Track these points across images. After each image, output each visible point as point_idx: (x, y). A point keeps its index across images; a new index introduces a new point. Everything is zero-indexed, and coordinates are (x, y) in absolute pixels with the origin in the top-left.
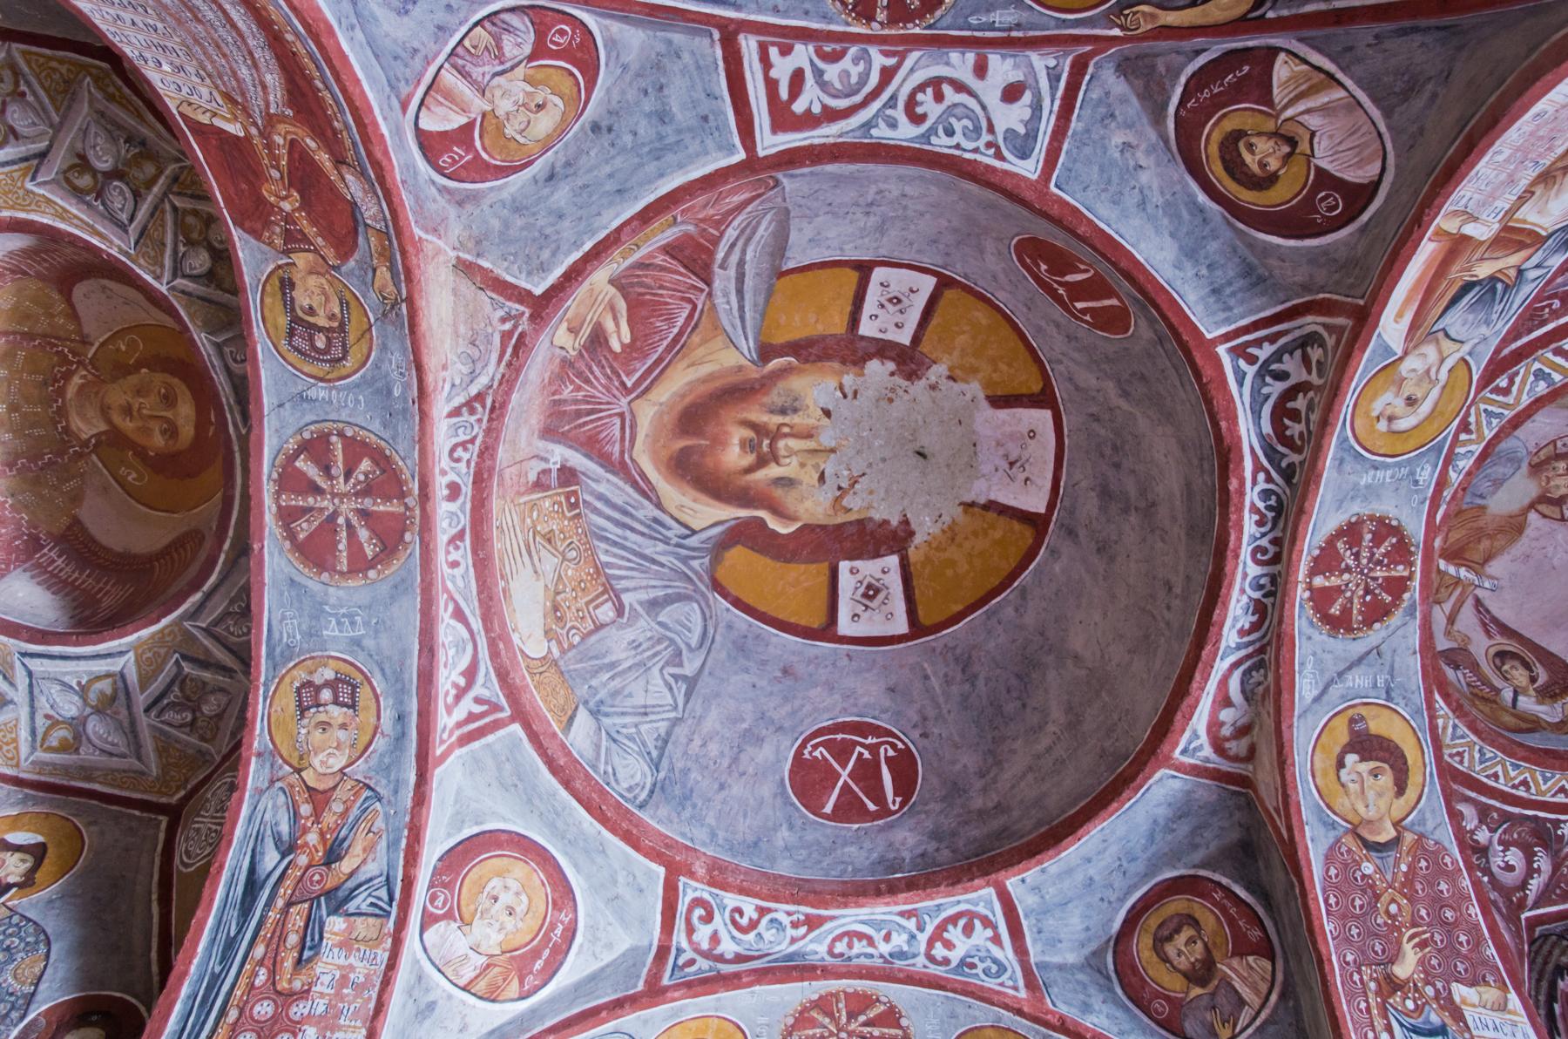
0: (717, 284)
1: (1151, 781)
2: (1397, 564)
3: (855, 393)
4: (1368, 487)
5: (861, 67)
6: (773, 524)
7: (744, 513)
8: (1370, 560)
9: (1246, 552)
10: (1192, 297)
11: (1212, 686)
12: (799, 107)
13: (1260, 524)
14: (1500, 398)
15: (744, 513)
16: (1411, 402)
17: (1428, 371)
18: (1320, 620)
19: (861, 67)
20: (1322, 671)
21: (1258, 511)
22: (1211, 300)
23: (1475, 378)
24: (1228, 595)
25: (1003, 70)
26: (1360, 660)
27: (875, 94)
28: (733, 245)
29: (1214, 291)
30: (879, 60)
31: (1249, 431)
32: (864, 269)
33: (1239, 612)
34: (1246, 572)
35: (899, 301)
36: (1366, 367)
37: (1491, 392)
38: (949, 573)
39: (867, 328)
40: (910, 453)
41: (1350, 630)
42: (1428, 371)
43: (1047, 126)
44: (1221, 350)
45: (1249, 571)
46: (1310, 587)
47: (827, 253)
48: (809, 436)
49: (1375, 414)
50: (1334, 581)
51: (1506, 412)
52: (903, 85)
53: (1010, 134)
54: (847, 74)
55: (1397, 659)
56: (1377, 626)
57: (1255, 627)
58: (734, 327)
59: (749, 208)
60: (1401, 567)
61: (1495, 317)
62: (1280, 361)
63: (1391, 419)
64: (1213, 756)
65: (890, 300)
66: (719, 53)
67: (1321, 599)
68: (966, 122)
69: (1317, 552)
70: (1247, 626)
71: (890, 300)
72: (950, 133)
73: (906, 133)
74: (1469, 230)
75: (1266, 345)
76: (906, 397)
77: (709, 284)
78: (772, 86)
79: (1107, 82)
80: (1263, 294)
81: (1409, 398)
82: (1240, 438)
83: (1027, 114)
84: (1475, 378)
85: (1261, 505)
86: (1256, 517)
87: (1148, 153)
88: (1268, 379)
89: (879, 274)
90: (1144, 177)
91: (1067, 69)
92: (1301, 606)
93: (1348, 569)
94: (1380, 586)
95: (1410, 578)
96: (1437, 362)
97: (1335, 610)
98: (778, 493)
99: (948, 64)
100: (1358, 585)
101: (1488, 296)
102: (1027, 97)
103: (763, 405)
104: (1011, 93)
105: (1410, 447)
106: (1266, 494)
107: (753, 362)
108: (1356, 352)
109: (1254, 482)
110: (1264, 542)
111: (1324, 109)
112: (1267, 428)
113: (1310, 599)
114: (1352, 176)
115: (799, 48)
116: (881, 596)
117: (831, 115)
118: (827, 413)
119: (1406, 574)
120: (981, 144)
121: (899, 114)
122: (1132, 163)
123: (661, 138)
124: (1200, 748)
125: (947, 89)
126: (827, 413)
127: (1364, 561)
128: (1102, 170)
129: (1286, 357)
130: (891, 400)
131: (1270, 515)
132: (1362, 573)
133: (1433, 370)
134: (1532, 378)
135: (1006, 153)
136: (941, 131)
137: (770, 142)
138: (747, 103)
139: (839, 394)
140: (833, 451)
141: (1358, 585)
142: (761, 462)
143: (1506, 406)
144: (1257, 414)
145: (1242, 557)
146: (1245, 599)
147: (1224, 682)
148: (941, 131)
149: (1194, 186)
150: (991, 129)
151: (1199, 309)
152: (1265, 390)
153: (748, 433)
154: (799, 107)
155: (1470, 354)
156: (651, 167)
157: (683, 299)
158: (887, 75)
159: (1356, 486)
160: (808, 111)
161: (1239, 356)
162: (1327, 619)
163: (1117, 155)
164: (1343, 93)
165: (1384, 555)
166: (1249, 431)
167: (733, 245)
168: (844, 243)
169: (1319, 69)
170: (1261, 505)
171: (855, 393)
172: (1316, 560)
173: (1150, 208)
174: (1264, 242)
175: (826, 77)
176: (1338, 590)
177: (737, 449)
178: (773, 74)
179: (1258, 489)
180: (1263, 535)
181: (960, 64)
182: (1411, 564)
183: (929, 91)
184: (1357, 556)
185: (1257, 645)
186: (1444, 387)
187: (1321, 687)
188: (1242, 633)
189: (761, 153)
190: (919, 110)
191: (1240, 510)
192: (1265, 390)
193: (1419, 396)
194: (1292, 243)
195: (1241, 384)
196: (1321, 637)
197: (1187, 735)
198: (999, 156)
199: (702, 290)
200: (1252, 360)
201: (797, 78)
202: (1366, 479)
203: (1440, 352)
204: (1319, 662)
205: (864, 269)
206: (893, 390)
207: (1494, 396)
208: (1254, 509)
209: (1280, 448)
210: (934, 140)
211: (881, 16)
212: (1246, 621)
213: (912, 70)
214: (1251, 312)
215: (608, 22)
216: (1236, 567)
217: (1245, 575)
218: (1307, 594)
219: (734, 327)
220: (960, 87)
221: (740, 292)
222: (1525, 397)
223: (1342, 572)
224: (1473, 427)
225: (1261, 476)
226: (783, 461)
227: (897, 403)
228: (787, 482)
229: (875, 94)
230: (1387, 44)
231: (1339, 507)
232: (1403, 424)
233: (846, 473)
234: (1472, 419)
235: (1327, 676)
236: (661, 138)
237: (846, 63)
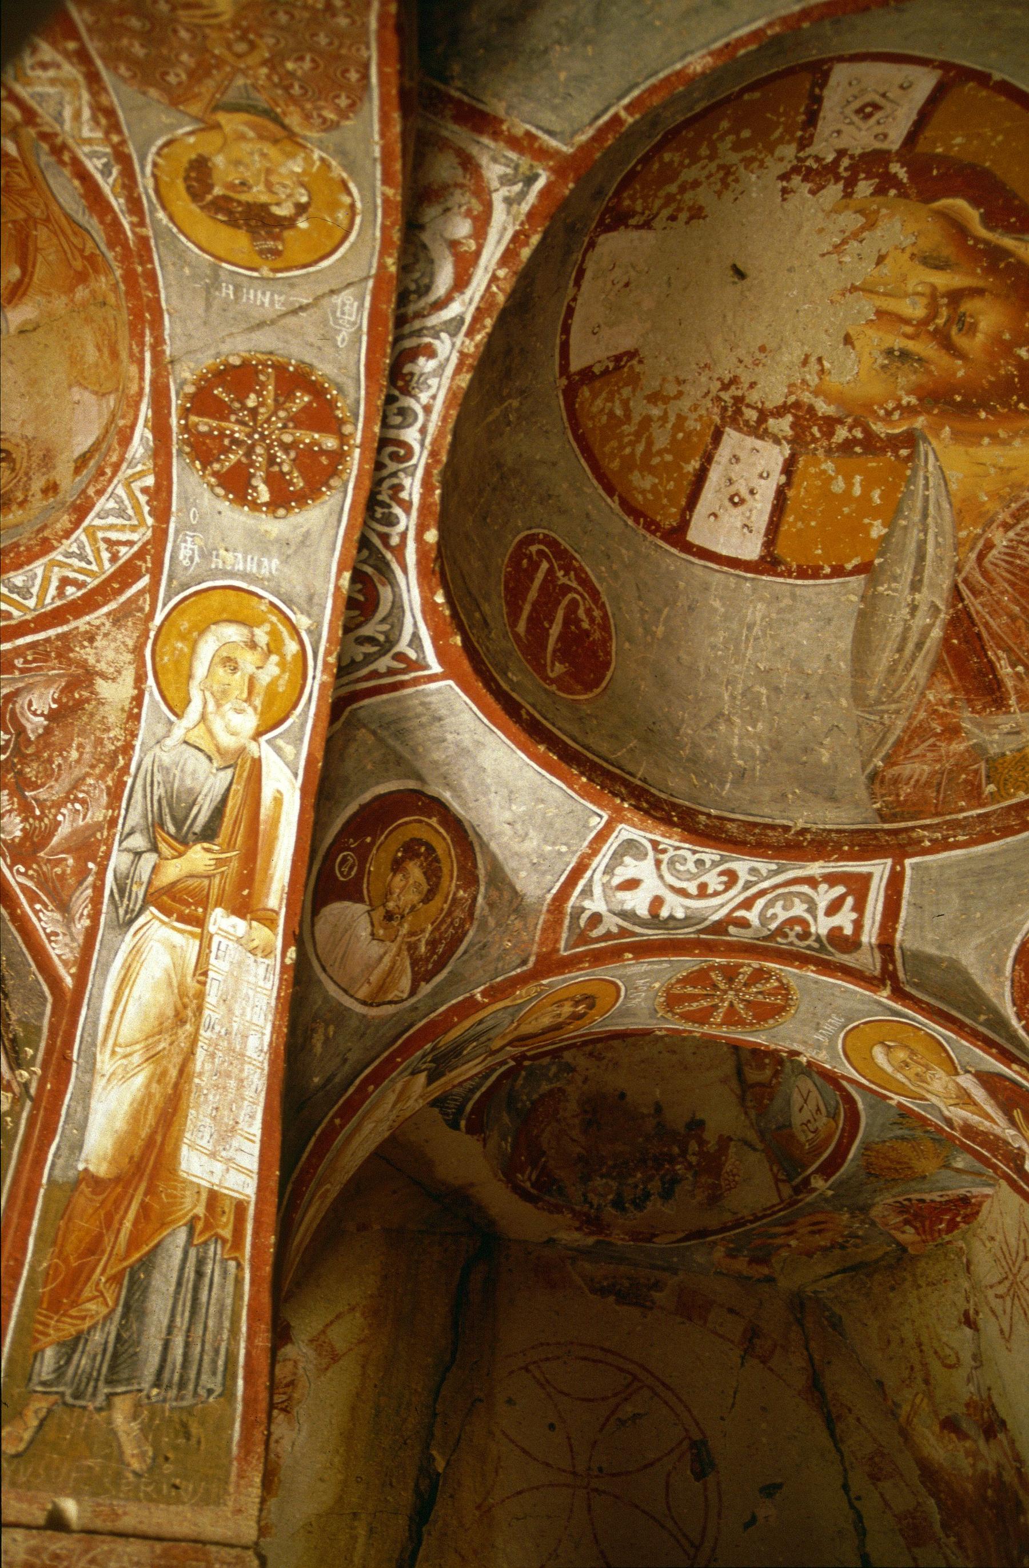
0: (946, 585)
1: (590, 132)
2: (209, 434)
3: (805, 363)
4: (265, 552)
5: (770, 912)
6: (972, 215)
7: (1008, 242)
8: (250, 451)
9: (420, 459)
10: (467, 716)
11: (480, 280)
12: (840, 890)
13: (398, 488)
14: (72, 575)
15: (1008, 242)
16: (231, 663)
17: (219, 705)
18: (326, 391)
19: (770, 912)
20: (325, 322)
21: (401, 503)
22: (443, 712)
23: (151, 681)
24: (448, 406)
25: (638, 902)
26: (261, 325)
27: (762, 893)
28: (919, 646)
29: (440, 719)
30: (752, 916)
31: (409, 588)
32: (769, 563)
33: (433, 382)
34: (424, 432)
35: (731, 499)
36: (303, 725)
37: (84, 584)
38: (746, 134)
39: (772, 457)
40: (751, 273)
41: (280, 369)
42: (219, 705)
43: (600, 861)
44: (436, 668)
45: (418, 436)
46: (343, 439)
47: (809, 593)
48: (880, 313)
49: (274, 658)
50: (307, 437)
51: (60, 558)
52: (736, 895)
53: (641, 856)
54: (784, 908)
55: (201, 311)
56: (235, 361)
57: (412, 355)
58: (939, 507)
59: (901, 723)
60: (204, 428)
61: (158, 777)
62: (366, 655)
63: (253, 645)
64: (484, 160)
65: (742, 501)
66: (898, 936)
67: (322, 415)
68: (681, 868)
69: (334, 482)
70: (422, 360)
71: (742, 501)
72: (700, 863)
73: (742, 866)
74: (239, 926)
75: (383, 670)
76: (741, 352)
77: (956, 587)
78: (859, 908)
79: (535, 885)
80: (384, 715)
81: (235, 670)
82: (420, 585)
83: (619, 870)
84: (151, 681)
85: (397, 510)
86: (404, 495)
87: (501, 833)
88: (382, 638)
89: (752, 550)
90: (507, 816)
91: (573, 899)
92: (356, 416)
93: (286, 448)
94: (234, 412)
95: (185, 413)
96: (210, 717)
97: (303, 399)
98: (948, 251)
99: (687, 908)
100: (268, 421)
101: (180, 815)
102: (616, 881)
103: (930, 373)
104: (632, 884)
105: (216, 596)
106: (391, 521)
107: (926, 440)
108: (320, 755)
109: (404, 535)
110: (392, 466)
111: (370, 968)
112: (386, 594)
113: (342, 422)
114: (337, 910)
115: (823, 931)
116: (857, 104)
117: (811, 882)
118: (848, 340)
119: (194, 419)
120: (671, 852)
121: (743, 876)
122: (518, 826)
123: (979, 882)
124: (506, 180)
125: (693, 890)
126: (848, 340)
127: (259, 450)
128: (551, 825)
129: (359, 658)
130: (762, 349)
131: (384, 497)
132: (263, 437)
133: (211, 706)
134: (35, 590)
135: (649, 846)
136: (708, 864)
137: (879, 869)
138: (888, 899)
139: (827, 365)
140: (854, 289)
141: (268, 421)
142: (955, 297)
143: (61, 565)
144: (397, 606)
145: (426, 453)
146: (424, 397)
147: (461, 283)
148: (708, 864)
149: (456, 806)
150: (658, 863)
151: (458, 706)
152: (385, 627)
153: (961, 341)
154: (840, 890)
155: (171, 723)
156: (998, 861)
157: (991, 582)
158: (747, 904)
159: (286, 560)
160: (832, 885)
161: (416, 662)
162: (317, 390)
163: (532, 833)
164: (360, 995)
165: (227, 451)
166: (409, 588)
167: (919, 646)
168: (791, 609)
169: (379, 1005)
170: (397, 510)
171: (805, 363)
172: (334, 473)
173: (505, 792)
174: (389, 779)
175: (805, 906)
176: (298, 421)
177: (983, 325)
178: (854, 916)
179: (401, 527)
180: (394, 474)
181: (675, 907)
182: (185, 429)
183: (710, 891)
184: (271, 460)
185: (407, 329)
186: (190, 677)
187: (324, 302)
188: (430, 353)
189: (889, 862)
190: (725, 879)
191: (424, 507)
192: (385, 627)
193: (220, 671)
194: (367, 797)
195: (416, 636)
196: (324, 369)
197: (525, 207)
198: (655, 844)
199: (965, 581)
200: (400, 657)
201: (834, 908)
202: (272, 565)
203: (210, 732)
204: (328, 338)
205: (769, 563)
206: (756, 363)
207: (81, 578)
208: (407, 506)
209: (369, 570)
210: (717, 858)
211: (748, 970)
212: (425, 365)
213: (722, 905)
214: (398, 700)
215: (995, 1000)
216: (434, 442)
217: (423, 431)
218: (347, 429)
219: (939, 507)
220: (683, 893)
221: (921, 557)
222: (40, 572)
223: (294, 445)
224: (103, 546)
225: (395, 541)
226: (928, 291)
227: (754, 348)
228: (933, 262)
229: (762, 893)
230: (338, 1060)
231: (307, 535)
232: (233, 633)
233: (847, 259)
234: (106, 555)
235: (314, 314)
236: (979, 882)
237: (783, 916)
